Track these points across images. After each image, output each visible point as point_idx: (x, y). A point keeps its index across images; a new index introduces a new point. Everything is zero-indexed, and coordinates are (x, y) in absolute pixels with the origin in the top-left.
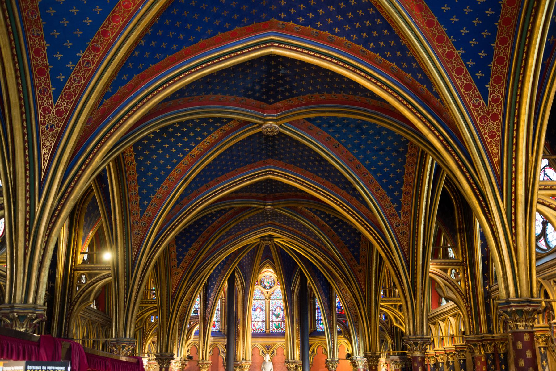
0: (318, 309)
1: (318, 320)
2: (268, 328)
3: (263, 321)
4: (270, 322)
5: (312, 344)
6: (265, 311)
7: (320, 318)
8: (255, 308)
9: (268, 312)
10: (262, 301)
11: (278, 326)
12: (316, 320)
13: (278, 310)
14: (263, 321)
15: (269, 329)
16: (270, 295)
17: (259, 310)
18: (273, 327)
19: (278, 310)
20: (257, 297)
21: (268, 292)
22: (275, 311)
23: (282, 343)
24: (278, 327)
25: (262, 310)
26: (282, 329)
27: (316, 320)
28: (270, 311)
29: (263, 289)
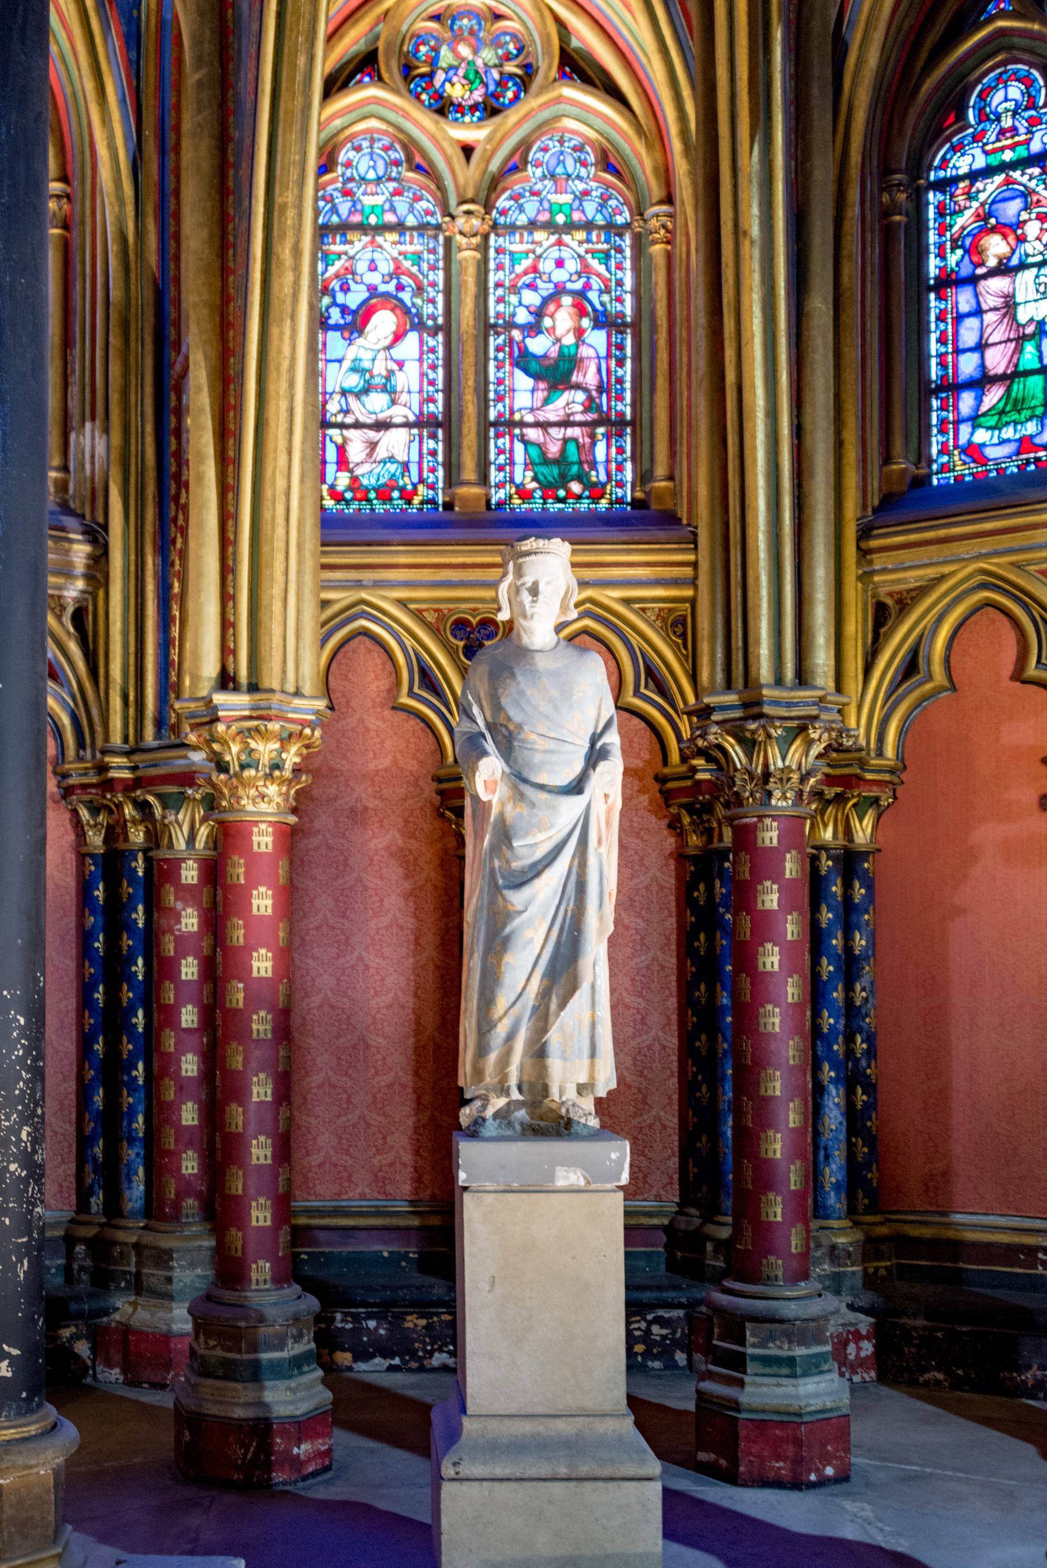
0: (948, 281)
1: (953, 387)
2: (469, 472)
3: (423, 423)
4: (485, 425)
5: (905, 602)
6: (447, 329)
7: (968, 365)
8: (354, 299)
9: (466, 341)
10: (415, 245)
11: (561, 461)
12: (926, 391)
13: (563, 320)
14: (423, 423)
15: (484, 479)
16: (494, 185)
17: (384, 322)
18: (513, 473)
19: (563, 320)
20: (373, 200)
21: (467, 150)
22: (534, 329)
23: (610, 596)
24: (559, 471)
25: (411, 321)
26: (596, 492)
27: (926, 391)
28: (486, 328)
29: (421, 123)
